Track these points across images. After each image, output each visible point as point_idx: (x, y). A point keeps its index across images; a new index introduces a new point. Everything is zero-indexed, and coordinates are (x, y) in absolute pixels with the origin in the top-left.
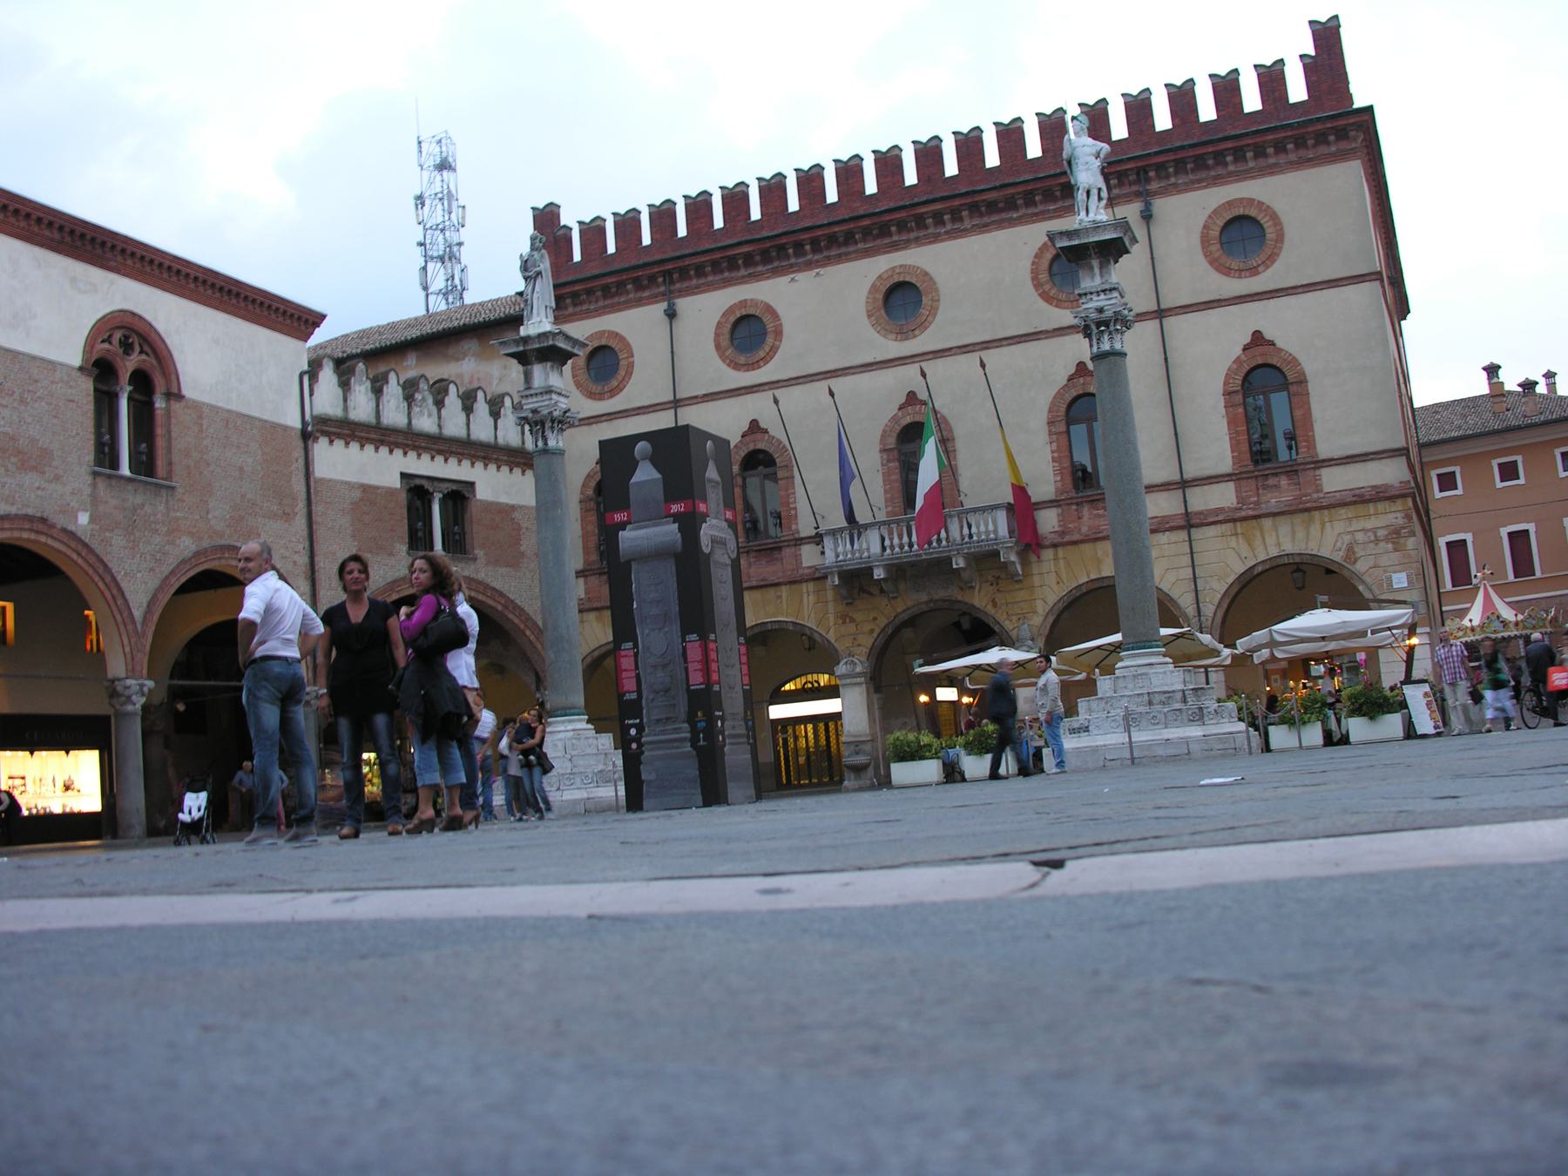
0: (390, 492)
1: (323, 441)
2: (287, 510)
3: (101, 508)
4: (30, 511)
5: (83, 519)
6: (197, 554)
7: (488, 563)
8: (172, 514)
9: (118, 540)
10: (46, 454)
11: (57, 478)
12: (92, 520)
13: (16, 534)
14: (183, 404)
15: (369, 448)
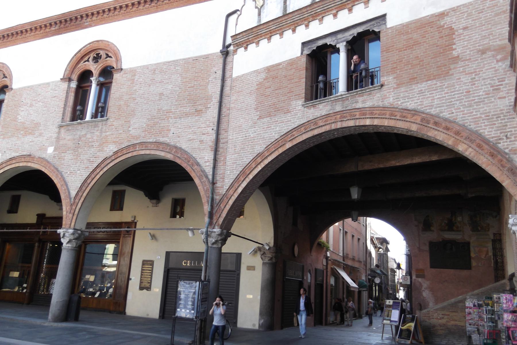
0: (291, 63)
1: (241, 50)
2: (200, 107)
3: (61, 142)
4: (25, 153)
5: (50, 150)
6: (116, 153)
7: (399, 85)
8: (104, 134)
9: (68, 157)
10: (38, 125)
11: (40, 135)
12: (55, 150)
13: (17, 165)
14: (122, 72)
15: (276, 38)
